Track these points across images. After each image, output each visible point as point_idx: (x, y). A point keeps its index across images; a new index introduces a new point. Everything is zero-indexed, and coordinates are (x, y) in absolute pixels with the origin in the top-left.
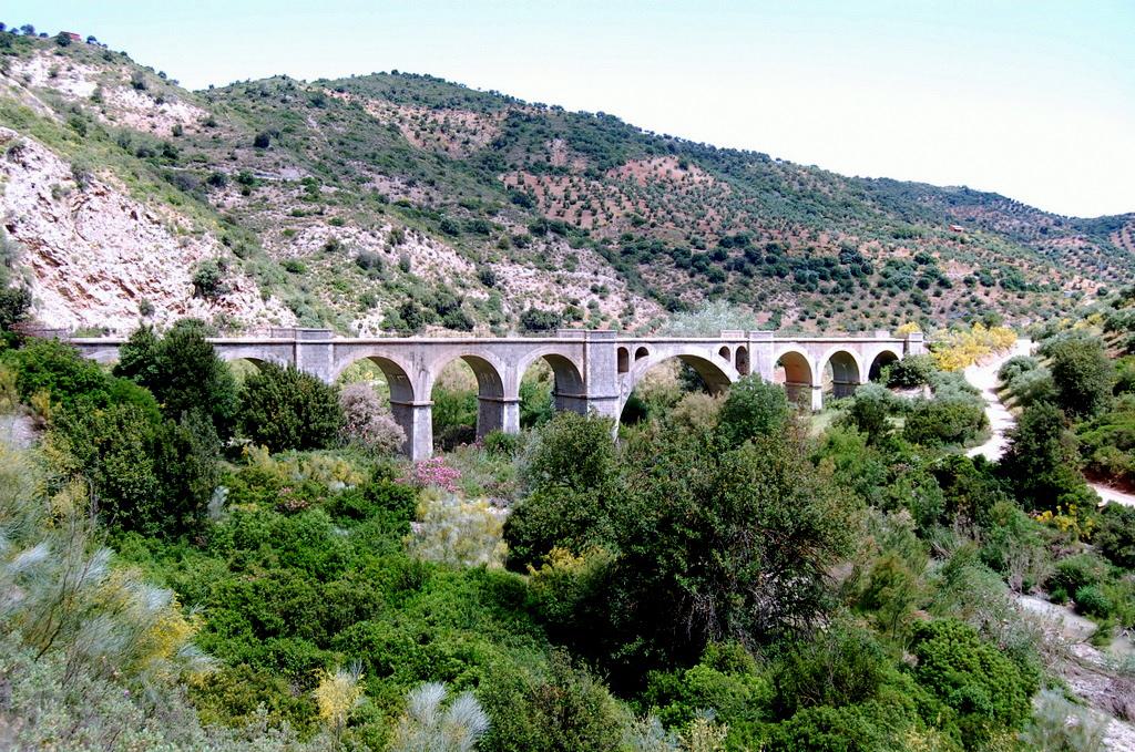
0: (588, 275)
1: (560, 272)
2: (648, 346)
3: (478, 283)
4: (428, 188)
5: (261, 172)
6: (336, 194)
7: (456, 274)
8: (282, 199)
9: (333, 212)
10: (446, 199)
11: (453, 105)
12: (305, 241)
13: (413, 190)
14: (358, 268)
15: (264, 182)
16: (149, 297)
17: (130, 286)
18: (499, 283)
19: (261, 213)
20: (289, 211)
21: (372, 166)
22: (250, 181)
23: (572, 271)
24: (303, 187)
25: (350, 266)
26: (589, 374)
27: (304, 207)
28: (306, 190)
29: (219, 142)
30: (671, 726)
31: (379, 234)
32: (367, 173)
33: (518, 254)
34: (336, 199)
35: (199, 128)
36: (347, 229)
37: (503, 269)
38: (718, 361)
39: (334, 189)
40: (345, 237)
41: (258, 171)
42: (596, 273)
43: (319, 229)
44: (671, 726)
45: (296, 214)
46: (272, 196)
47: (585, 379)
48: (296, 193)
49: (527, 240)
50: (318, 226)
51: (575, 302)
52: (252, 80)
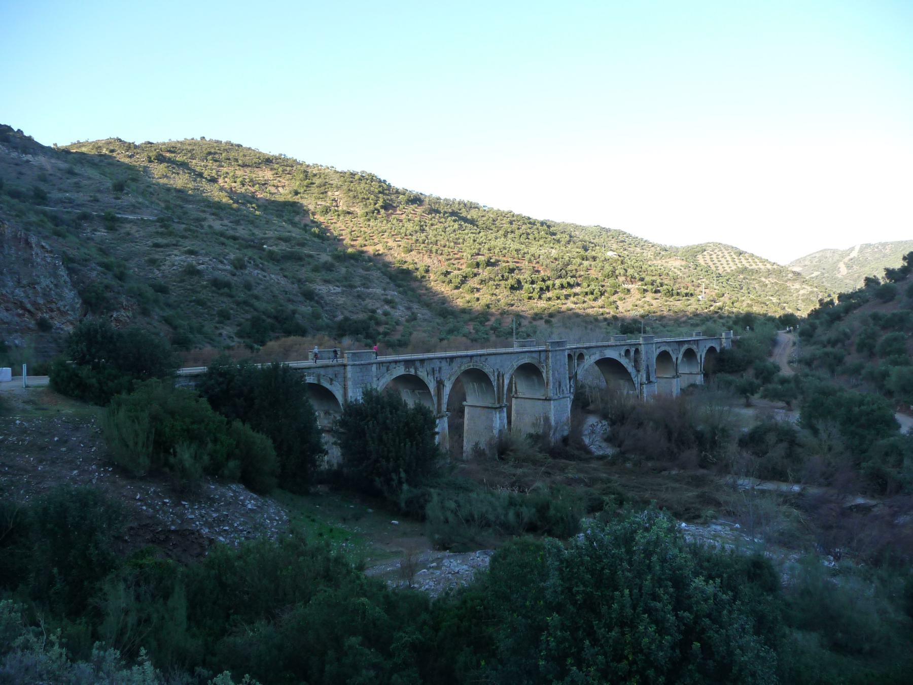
0: (379, 291)
1: (359, 289)
3: (301, 298)
5: (122, 212)
6: (186, 230)
7: (286, 293)
8: (142, 233)
9: (188, 244)
10: (265, 234)
11: (258, 166)
13: (240, 228)
14: (214, 288)
15: (127, 221)
16: (46, 316)
17: (29, 306)
20: (150, 243)
21: (206, 209)
22: (113, 219)
23: (368, 288)
26: (551, 378)
27: (160, 240)
28: (161, 227)
29: (79, 187)
31: (225, 262)
34: (186, 234)
35: (60, 176)
36: (200, 257)
37: (318, 287)
38: (624, 361)
39: (184, 226)
40: (200, 264)
42: (385, 290)
43: (177, 258)
45: (157, 245)
46: (133, 231)
47: (548, 380)
48: (152, 229)
49: (332, 265)
50: (176, 255)
51: (374, 311)
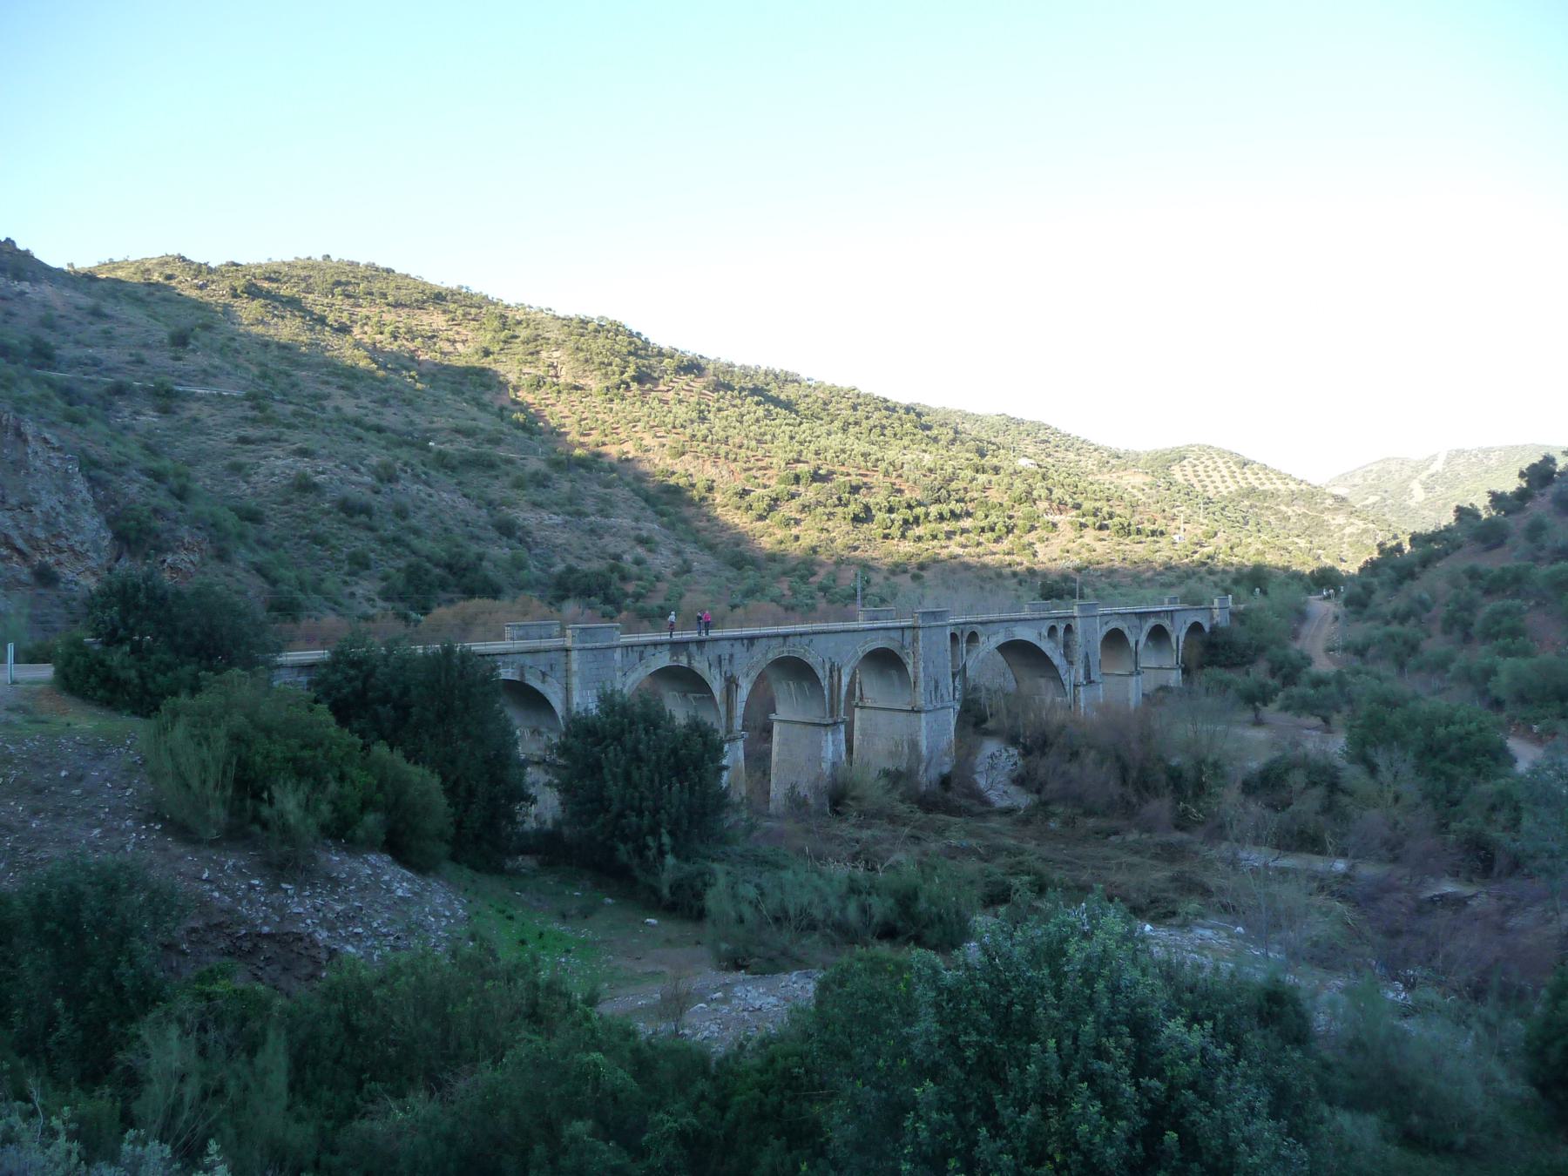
0: (627, 522)
1: (592, 518)
2: (978, 629)
3: (494, 534)
4: (407, 410)
5: (183, 382)
6: (295, 414)
7: (467, 524)
8: (219, 419)
9: (298, 439)
10: (432, 422)
11: (421, 305)
12: (261, 478)
13: (388, 412)
14: (342, 515)
15: (191, 397)
16: (50, 560)
17: (20, 543)
18: (519, 534)
19: (191, 439)
20: (232, 436)
21: (330, 379)
22: (170, 394)
23: (607, 517)
24: (248, 404)
25: (328, 513)
26: (921, 675)
27: (250, 432)
28: (253, 408)
29: (112, 338)
30: (1146, 1122)
31: (363, 469)
32: (321, 387)
33: (540, 496)
34: (296, 421)
35: (78, 318)
36: (319, 462)
37: (523, 515)
38: (1046, 646)
39: (291, 407)
40: (320, 473)
41: (178, 381)
42: (637, 520)
43: (279, 462)
44: (1146, 1122)
45: (244, 440)
46: (203, 416)
47: (916, 677)
48: (237, 412)
49: (547, 477)
50: (277, 458)
51: (618, 557)
52: (335, 258)
